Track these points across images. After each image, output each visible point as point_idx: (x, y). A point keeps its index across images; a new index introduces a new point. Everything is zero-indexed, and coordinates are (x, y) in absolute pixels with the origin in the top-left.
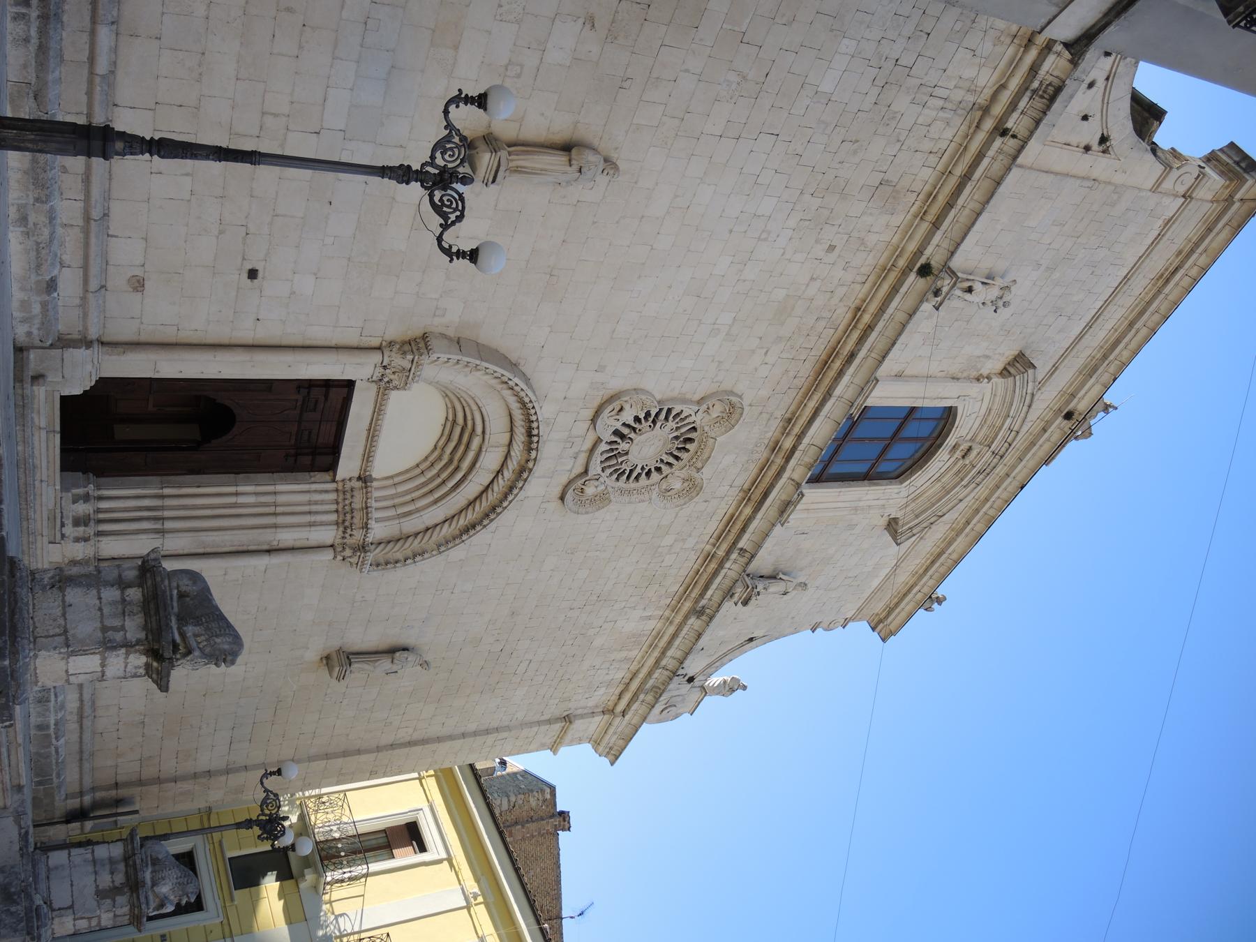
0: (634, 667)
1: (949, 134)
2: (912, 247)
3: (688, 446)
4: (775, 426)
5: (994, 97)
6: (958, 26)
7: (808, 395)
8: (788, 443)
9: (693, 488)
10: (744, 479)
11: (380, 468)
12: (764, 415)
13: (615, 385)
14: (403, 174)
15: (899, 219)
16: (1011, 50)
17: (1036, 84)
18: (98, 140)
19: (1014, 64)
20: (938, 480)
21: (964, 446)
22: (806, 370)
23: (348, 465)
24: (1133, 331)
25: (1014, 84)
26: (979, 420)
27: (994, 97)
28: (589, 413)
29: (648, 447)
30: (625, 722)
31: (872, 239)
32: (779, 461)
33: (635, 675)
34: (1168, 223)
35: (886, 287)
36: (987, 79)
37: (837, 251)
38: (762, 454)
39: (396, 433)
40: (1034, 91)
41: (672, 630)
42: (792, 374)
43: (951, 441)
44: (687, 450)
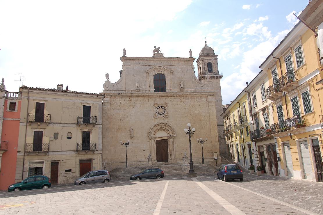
9: (166, 103)
10: (165, 98)
11: (167, 135)
13: (153, 117)
14: (126, 146)
18: (126, 163)
23: (166, 139)
28: (156, 119)
29: (161, 111)
36: (119, 98)
38: (161, 97)
39: (162, 135)
43: (159, 73)
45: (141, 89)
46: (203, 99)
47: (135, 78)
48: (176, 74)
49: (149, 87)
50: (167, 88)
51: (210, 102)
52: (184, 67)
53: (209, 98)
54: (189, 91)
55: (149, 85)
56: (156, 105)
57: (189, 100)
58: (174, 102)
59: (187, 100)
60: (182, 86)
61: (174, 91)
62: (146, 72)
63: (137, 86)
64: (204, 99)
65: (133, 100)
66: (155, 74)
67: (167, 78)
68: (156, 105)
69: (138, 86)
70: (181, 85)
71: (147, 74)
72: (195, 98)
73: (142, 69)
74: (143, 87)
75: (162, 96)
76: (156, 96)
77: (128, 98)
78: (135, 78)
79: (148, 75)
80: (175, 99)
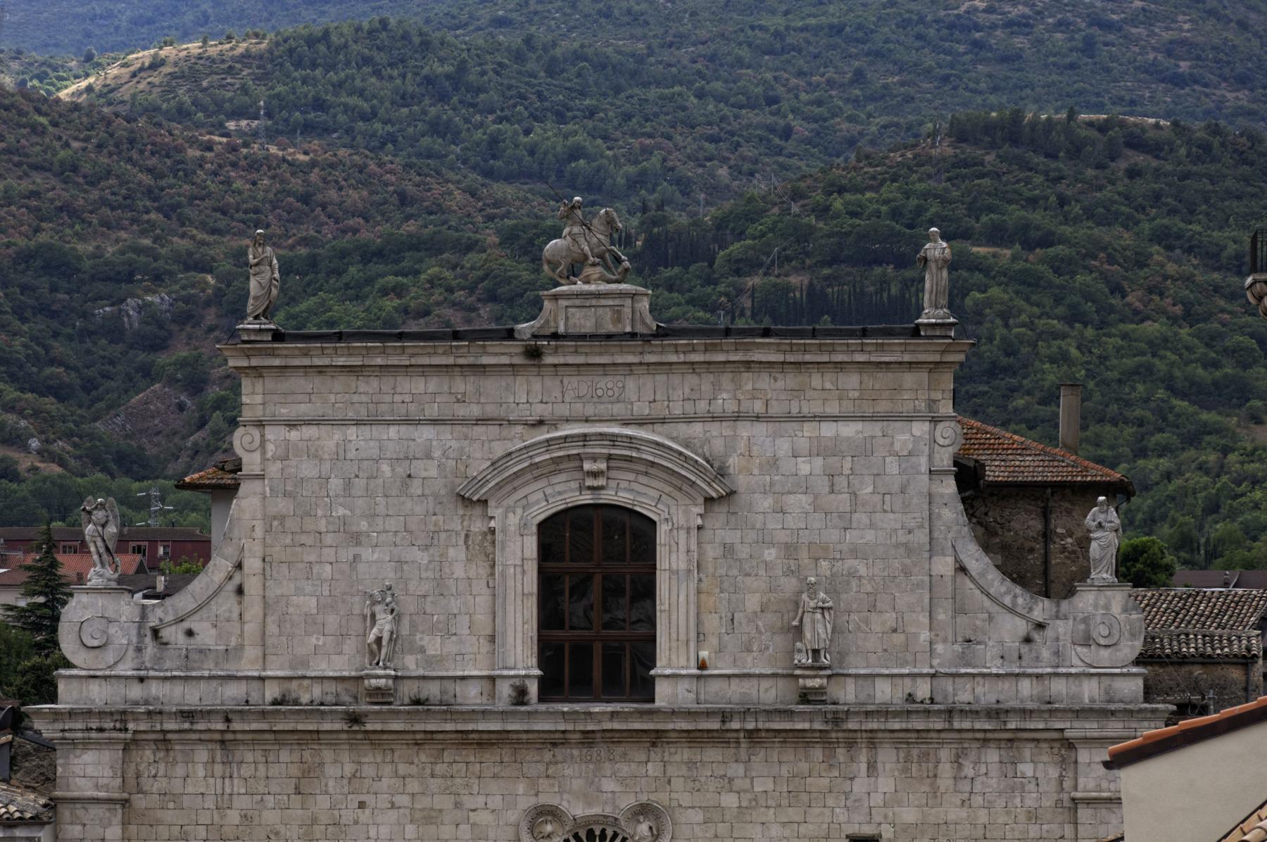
0: (976, 745)
1: (249, 757)
2: (344, 736)
3: (597, 833)
4: (560, 752)
5: (211, 741)
6: (171, 805)
7: (519, 742)
8: (577, 736)
9: (644, 810)
12: (550, 772)
15: (328, 755)
16: (177, 747)
17: (187, 726)
19: (183, 742)
20: (646, 473)
21: (590, 482)
22: (491, 756)
24: (413, 361)
25: (194, 736)
26: (555, 480)
27: (211, 741)
30: (1077, 724)
31: (349, 769)
32: (598, 735)
33: (985, 740)
34: (292, 424)
35: (385, 737)
36: (202, 754)
37: (362, 798)
38: (601, 751)
40: (192, 723)
41: (880, 735)
42: (497, 769)
43: (587, 498)
44: (603, 831)
45: (411, 664)
46: (1026, 769)
47: (356, 558)
48: (766, 503)
49: (485, 647)
50: (671, 658)
51: (1089, 802)
52: (849, 430)
53: (1083, 756)
54: (884, 692)
55: (489, 629)
56: (549, 828)
57: (886, 784)
58: (730, 800)
59: (860, 786)
60: (817, 630)
61: (735, 691)
62: (465, 501)
63: (372, 637)
64: (1038, 769)
65: (337, 766)
66: (557, 506)
67: (671, 558)
68: (549, 828)
69: (379, 640)
70: (799, 631)
71: (478, 511)
72: (945, 754)
73: (428, 456)
74: (433, 646)
75: (613, 738)
76: (555, 741)
77: (285, 755)
78: (356, 558)
79: (478, 526)
80: (739, 770)
